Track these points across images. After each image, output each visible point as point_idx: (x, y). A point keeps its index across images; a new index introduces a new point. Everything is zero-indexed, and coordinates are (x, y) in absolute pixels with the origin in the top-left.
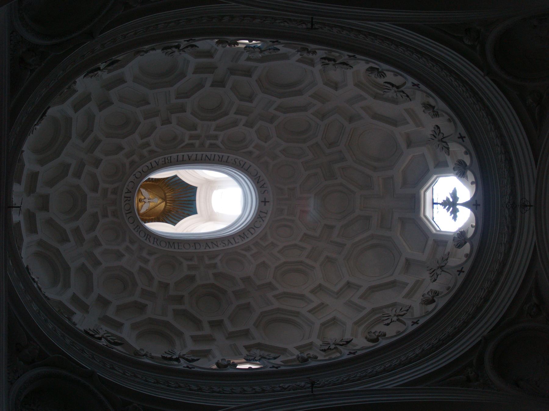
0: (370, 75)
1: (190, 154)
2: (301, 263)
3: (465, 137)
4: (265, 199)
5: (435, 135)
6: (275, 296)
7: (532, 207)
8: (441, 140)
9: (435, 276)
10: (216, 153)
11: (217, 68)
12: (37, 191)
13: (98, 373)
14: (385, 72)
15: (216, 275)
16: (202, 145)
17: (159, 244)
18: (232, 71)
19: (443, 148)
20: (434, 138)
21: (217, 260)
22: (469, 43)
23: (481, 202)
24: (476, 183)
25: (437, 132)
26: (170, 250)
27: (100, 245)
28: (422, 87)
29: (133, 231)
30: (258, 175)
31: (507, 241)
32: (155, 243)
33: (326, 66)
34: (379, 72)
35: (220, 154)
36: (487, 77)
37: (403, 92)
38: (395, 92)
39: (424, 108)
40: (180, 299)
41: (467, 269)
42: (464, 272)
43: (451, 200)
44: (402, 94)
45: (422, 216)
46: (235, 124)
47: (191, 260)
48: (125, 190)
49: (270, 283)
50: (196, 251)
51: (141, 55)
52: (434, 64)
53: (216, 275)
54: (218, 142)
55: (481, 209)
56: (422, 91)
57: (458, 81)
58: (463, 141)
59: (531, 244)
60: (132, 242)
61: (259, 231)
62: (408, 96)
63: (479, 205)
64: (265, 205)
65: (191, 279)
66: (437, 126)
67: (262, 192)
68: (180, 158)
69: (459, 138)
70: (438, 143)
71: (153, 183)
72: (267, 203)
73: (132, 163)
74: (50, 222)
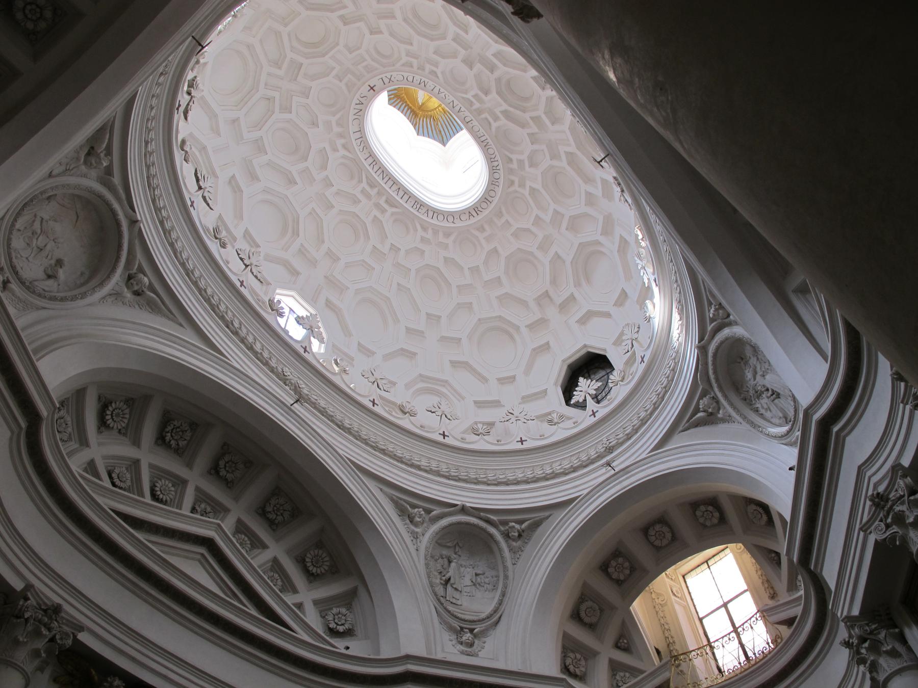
1: (394, 195)
2: (405, 20)
4: (369, 91)
6: (467, 33)
10: (373, 174)
11: (325, 277)
12: (540, 316)
13: (697, 343)
15: (486, 93)
16: (379, 194)
17: (493, 156)
21: (469, 96)
22: (146, 279)
26: (491, 142)
27: (538, 218)
29: (501, 186)
30: (356, 117)
32: (496, 159)
34: (220, 239)
35: (370, 169)
36: (139, 219)
40: (537, 120)
47: (486, 119)
48: (473, 220)
49: (454, 40)
50: (473, 119)
53: (486, 93)
54: (364, 184)
60: (512, 183)
61: (406, 75)
64: (375, 86)
65: (505, 113)
67: (365, 98)
68: (406, 197)
71: (406, 99)
72: (372, 86)
73: (447, 235)
74: (554, 281)
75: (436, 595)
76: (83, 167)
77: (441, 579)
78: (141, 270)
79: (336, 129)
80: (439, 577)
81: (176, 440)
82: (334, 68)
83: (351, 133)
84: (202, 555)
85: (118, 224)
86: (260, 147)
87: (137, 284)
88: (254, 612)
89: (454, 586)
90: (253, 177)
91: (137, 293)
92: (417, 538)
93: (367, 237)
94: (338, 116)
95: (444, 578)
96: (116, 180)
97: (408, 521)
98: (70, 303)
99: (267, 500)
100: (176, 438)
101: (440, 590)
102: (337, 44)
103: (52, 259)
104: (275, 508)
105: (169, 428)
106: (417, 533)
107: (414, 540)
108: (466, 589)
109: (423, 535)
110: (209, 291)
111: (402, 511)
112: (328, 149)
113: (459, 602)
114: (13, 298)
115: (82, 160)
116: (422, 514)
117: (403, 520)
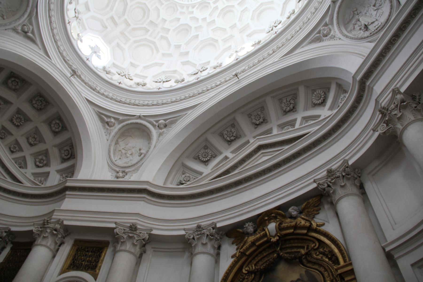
0: (181, 78)
3: (119, 84)
5: (129, 76)
7: (70, 76)
8: (125, 75)
9: (76, 11)
11: (240, 33)
14: (177, 84)
18: (232, 37)
19: (121, 72)
20: (129, 74)
23: (87, 62)
24: (96, 68)
25: (130, 78)
28: (156, 90)
31: (63, 53)
33: (202, 67)
34: (179, 81)
36: (139, 114)
37: (160, 82)
38: (162, 80)
39: (145, 82)
41: (68, 25)
42: (68, 23)
43: (98, 54)
44: (160, 81)
45: (99, 37)
46: (210, 15)
51: (290, 12)
52: (163, 102)
55: (85, 59)
56: (155, 88)
57: (147, 104)
58: (118, 82)
59: (53, 59)
62: (156, 82)
63: (87, 60)
66: (132, 80)
69: (120, 82)
70: (125, 73)
75: (362, 38)
76: (111, 128)
77: (363, 30)
78: (157, 121)
79: (184, 10)
80: (362, 31)
81: (232, 136)
82: (157, 7)
83: (188, 3)
84: (262, 153)
85: (137, 123)
86: (178, 47)
87: (161, 125)
88: (286, 147)
89: (370, 24)
90: (187, 53)
91: (165, 126)
92: (334, 36)
93: (233, 6)
94: (179, 7)
95: (363, 28)
96: (121, 118)
97: (325, 38)
98: (148, 154)
99: (282, 108)
100: (231, 136)
101: (367, 34)
102: (145, 4)
103: (137, 152)
104: (288, 106)
105: (225, 136)
106: (332, 35)
107: (335, 38)
108: (377, 16)
109: (335, 32)
110: (187, 96)
111: (318, 40)
112: (191, 16)
113: (380, 24)
114: (132, 172)
115: (108, 127)
116: (324, 29)
117: (323, 41)
